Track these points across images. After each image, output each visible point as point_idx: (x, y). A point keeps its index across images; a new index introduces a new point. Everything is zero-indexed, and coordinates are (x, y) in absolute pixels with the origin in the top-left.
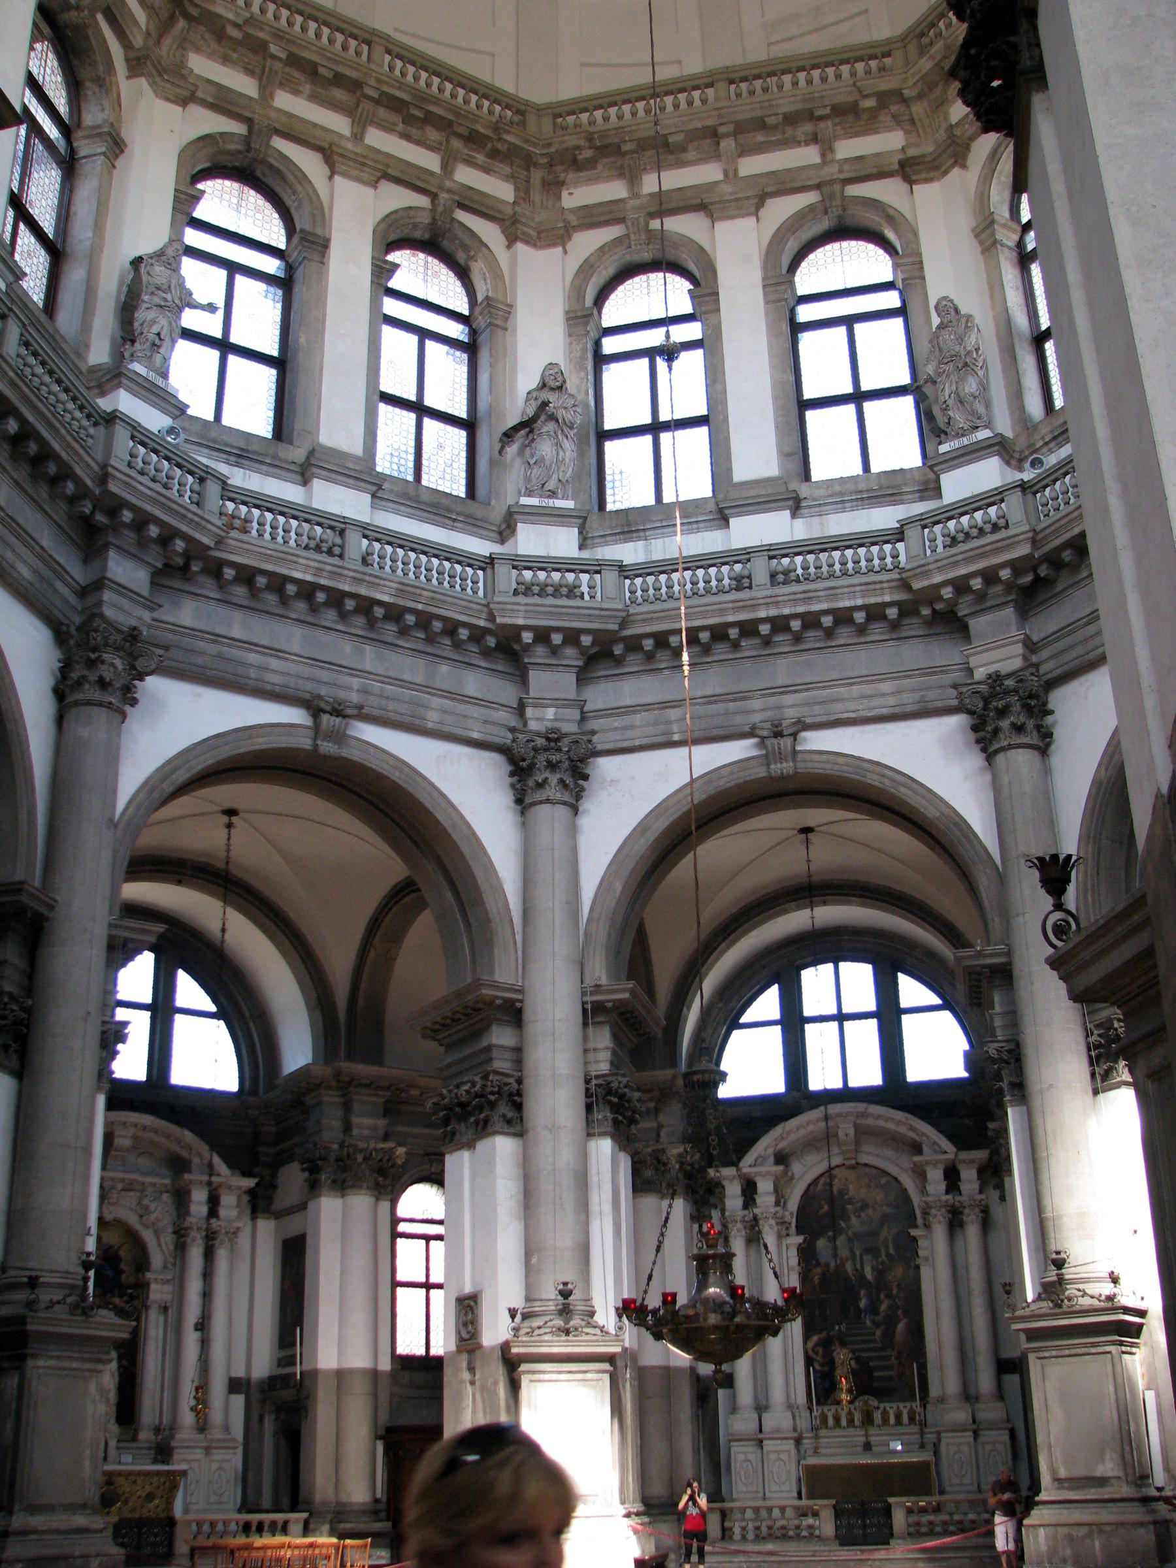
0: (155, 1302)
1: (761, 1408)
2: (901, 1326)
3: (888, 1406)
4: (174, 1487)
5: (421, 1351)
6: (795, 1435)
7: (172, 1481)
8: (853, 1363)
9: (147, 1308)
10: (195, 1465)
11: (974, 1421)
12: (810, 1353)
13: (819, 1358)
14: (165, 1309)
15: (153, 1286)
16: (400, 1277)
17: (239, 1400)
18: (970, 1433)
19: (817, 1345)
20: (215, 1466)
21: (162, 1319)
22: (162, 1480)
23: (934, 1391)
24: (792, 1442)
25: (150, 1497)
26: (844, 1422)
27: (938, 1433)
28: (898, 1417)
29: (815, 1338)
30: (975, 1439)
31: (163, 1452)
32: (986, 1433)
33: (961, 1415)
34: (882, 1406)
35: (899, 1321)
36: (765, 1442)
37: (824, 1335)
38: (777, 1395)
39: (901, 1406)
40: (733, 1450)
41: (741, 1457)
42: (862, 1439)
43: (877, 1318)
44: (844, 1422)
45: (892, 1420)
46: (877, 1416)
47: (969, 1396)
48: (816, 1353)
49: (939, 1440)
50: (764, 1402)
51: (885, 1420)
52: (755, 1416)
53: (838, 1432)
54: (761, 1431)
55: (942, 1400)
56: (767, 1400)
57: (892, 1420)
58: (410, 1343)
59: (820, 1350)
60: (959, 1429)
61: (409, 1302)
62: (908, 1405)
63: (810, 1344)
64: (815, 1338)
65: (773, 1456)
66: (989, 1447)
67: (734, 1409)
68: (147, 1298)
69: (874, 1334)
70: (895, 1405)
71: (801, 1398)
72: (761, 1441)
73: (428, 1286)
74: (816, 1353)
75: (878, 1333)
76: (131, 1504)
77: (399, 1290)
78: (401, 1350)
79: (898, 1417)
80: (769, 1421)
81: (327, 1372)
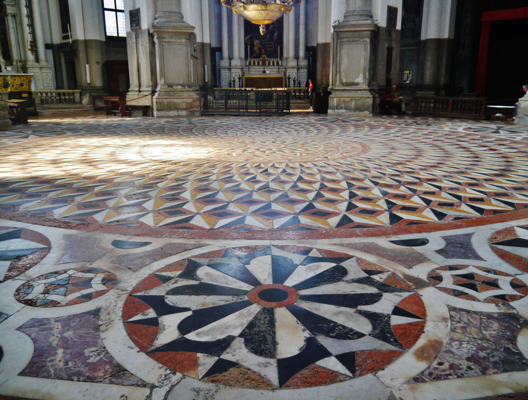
0: (10, 13)
1: (231, 58)
2: (276, 34)
3: (270, 59)
4: (30, 82)
5: (116, 35)
6: (241, 67)
7: (29, 79)
8: (260, 45)
9: (7, 15)
10: (37, 74)
11: (298, 65)
12: (246, 41)
13: (249, 43)
14: (14, 16)
15: (8, 7)
16: (105, 7)
17: (50, 52)
18: (296, 69)
19: (248, 39)
20: (44, 74)
21: (14, 20)
22: (25, 79)
23: (285, 56)
24: (240, 70)
25: (22, 85)
26: (256, 64)
27: (286, 69)
28: (273, 63)
29: (248, 37)
30: (297, 71)
31: (25, 69)
32: (301, 69)
33: (293, 63)
34: (269, 59)
35: (275, 32)
36: (232, 69)
37: (251, 36)
38: (236, 54)
39: (274, 60)
40: (221, 72)
41: (224, 74)
42: (262, 70)
43: (268, 31)
44: (256, 64)
45: (271, 64)
46: (267, 63)
47: (297, 57)
48: (248, 42)
49: (286, 70)
50: (231, 57)
51: (269, 64)
52: (229, 61)
53: (254, 67)
54: (230, 65)
55: (287, 59)
56: (233, 55)
57: (271, 64)
58: (111, 31)
59: (250, 41)
60: (293, 68)
61: (109, 16)
62: (277, 60)
63: (246, 38)
64: (248, 37)
65: (234, 74)
66: (302, 74)
67: (221, 58)
68: (6, 11)
69: (267, 36)
70: (273, 59)
71: (243, 56)
72: (230, 69)
73: (116, 11)
74: (248, 42)
75: (268, 36)
76: (14, 87)
77: (106, 12)
78: (108, 34)
79: (273, 63)
80: (233, 63)
81: (81, 41)
